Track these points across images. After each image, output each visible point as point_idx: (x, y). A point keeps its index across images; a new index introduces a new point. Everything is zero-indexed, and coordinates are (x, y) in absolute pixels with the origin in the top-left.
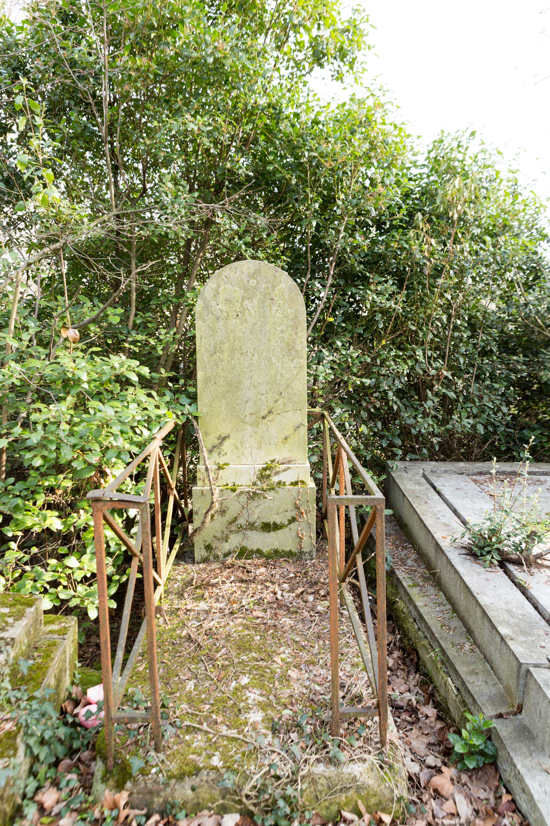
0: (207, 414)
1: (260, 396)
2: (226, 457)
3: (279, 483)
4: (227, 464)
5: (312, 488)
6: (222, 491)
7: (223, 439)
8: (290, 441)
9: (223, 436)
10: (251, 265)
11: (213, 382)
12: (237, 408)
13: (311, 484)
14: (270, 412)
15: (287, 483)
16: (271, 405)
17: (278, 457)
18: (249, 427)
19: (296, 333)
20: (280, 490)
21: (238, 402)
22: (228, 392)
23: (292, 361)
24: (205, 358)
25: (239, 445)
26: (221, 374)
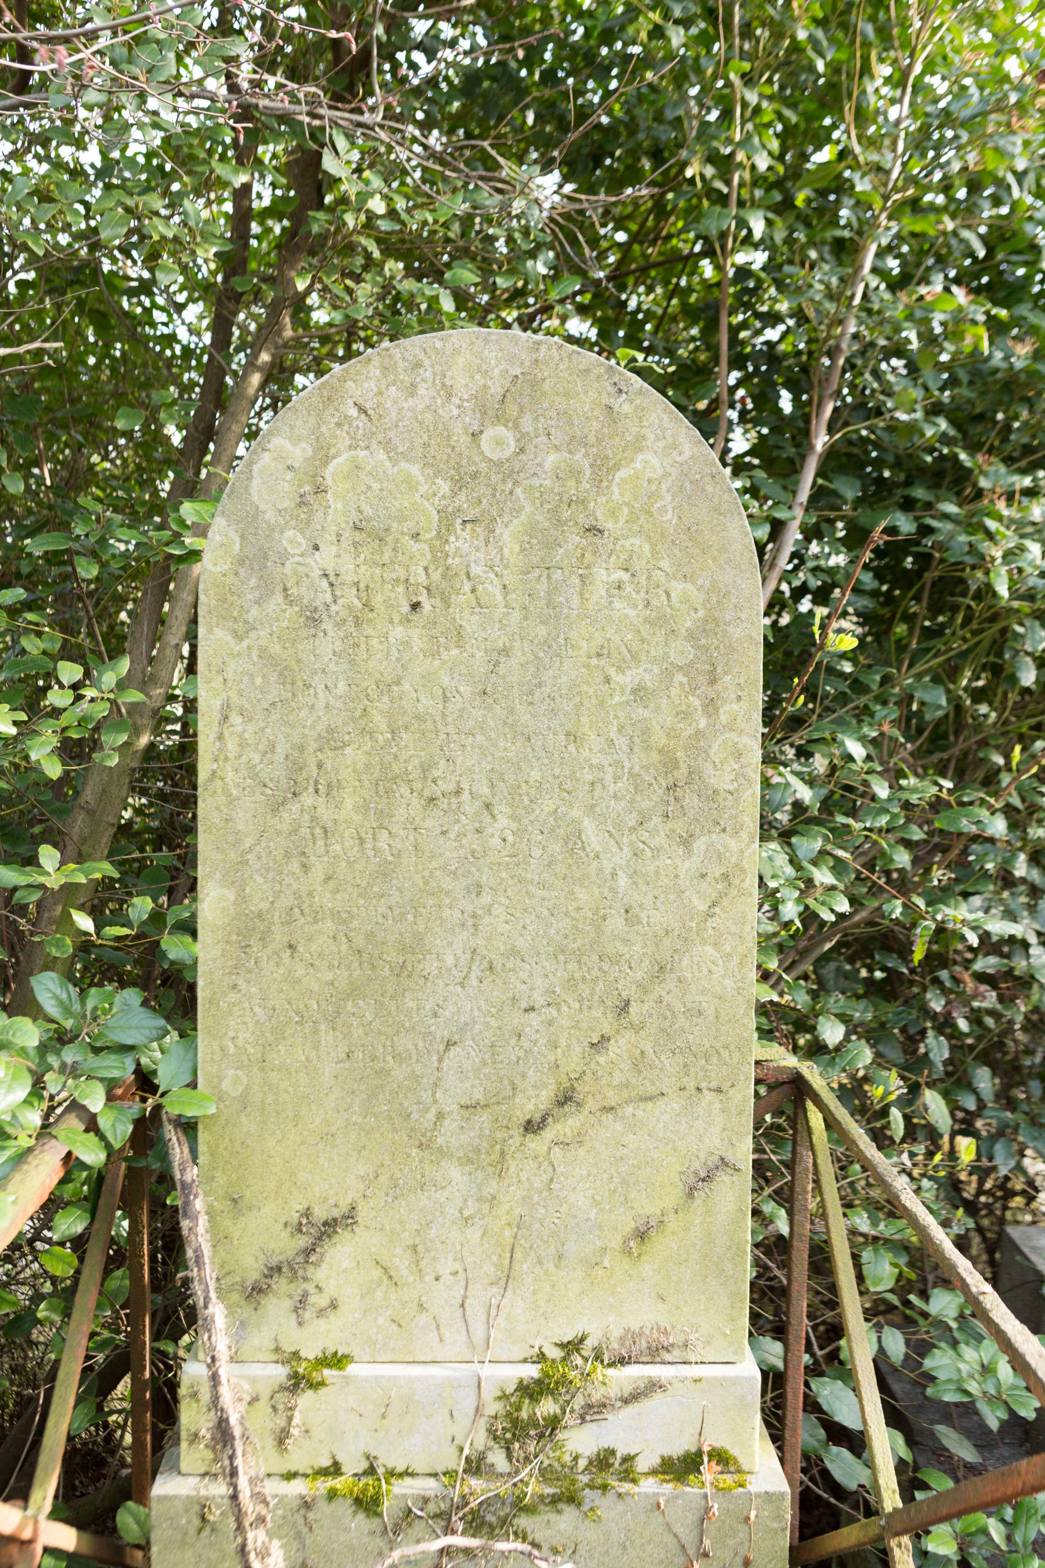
0: (244, 1102)
1: (517, 1019)
2: (335, 1321)
3: (603, 1461)
4: (337, 1361)
5: (769, 1497)
6: (306, 1505)
7: (323, 1231)
8: (661, 1245)
9: (321, 1214)
10: (492, 355)
11: (279, 937)
12: (399, 1073)
13: (767, 1474)
14: (566, 1099)
15: (642, 1465)
16: (573, 1062)
17: (599, 1327)
18: (456, 1173)
19: (711, 706)
20: (605, 1505)
21: (404, 1043)
22: (354, 991)
23: (686, 842)
24: (243, 820)
25: (401, 1264)
26: (325, 899)
